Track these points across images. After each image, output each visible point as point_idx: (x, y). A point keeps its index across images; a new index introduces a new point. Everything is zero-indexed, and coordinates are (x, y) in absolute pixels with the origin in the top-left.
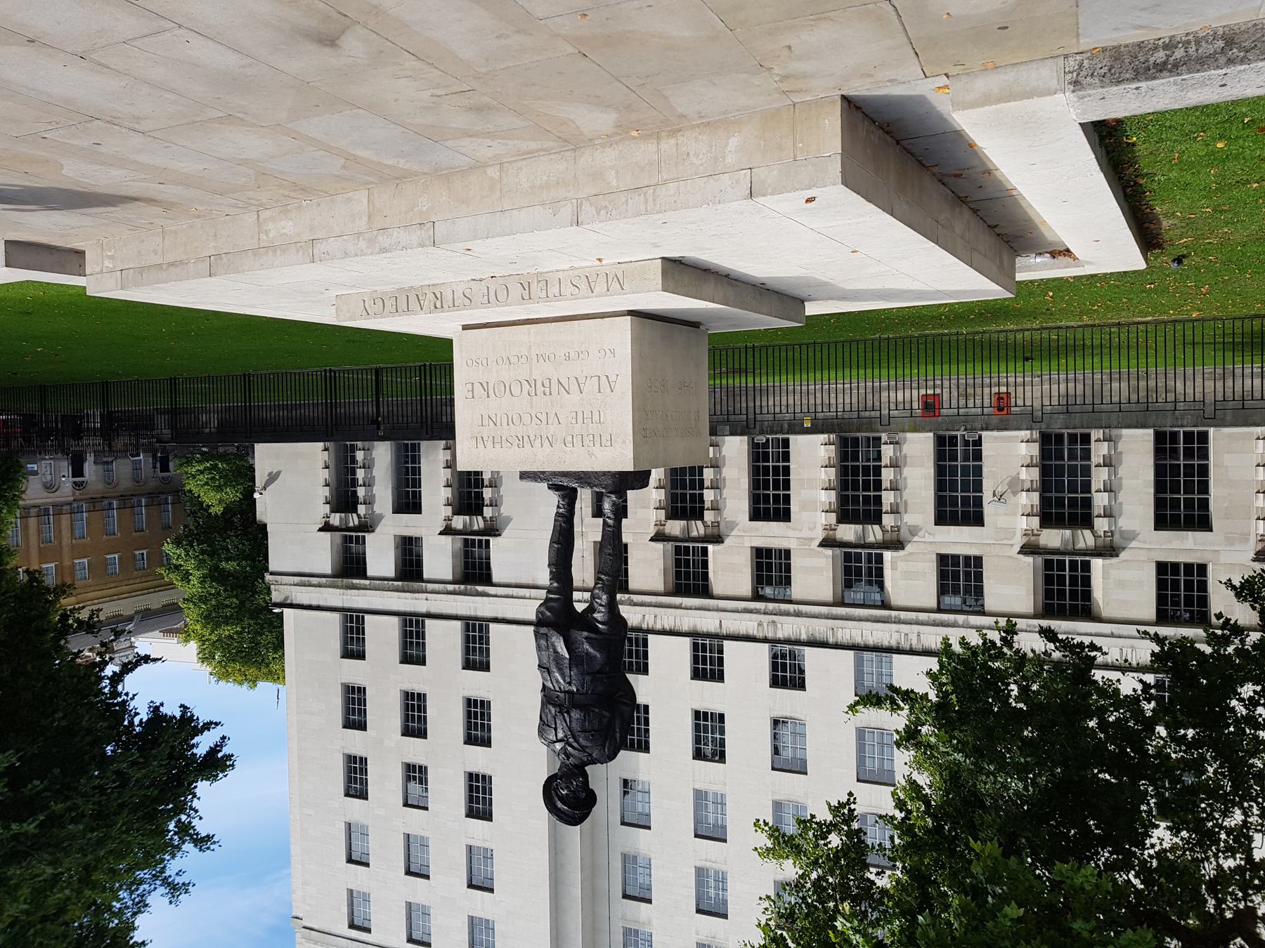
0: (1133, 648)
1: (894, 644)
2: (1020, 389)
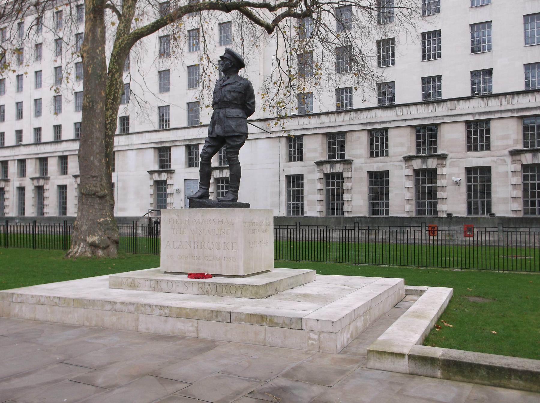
0: (398, 116)
1: (516, 97)
2: (424, 237)
